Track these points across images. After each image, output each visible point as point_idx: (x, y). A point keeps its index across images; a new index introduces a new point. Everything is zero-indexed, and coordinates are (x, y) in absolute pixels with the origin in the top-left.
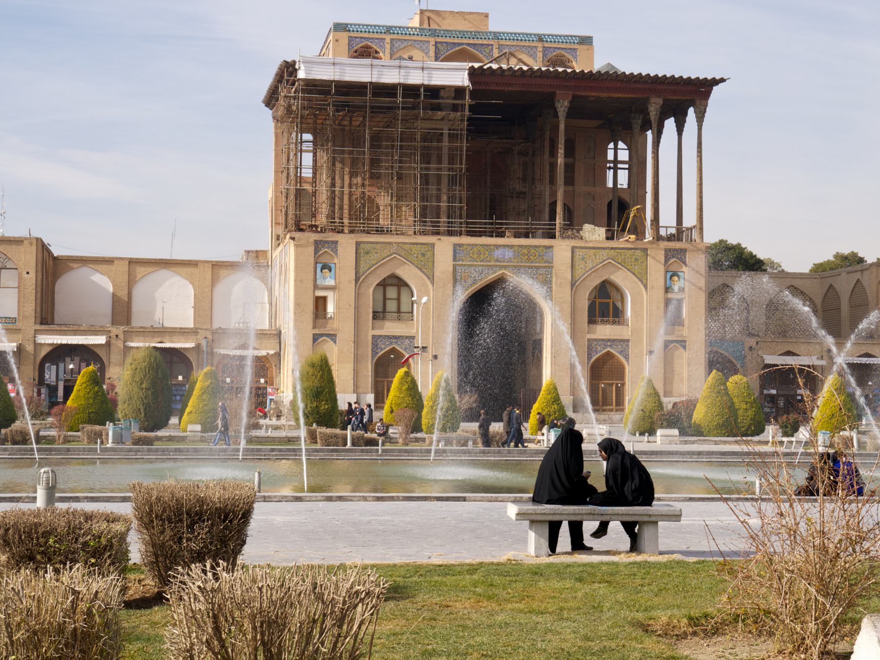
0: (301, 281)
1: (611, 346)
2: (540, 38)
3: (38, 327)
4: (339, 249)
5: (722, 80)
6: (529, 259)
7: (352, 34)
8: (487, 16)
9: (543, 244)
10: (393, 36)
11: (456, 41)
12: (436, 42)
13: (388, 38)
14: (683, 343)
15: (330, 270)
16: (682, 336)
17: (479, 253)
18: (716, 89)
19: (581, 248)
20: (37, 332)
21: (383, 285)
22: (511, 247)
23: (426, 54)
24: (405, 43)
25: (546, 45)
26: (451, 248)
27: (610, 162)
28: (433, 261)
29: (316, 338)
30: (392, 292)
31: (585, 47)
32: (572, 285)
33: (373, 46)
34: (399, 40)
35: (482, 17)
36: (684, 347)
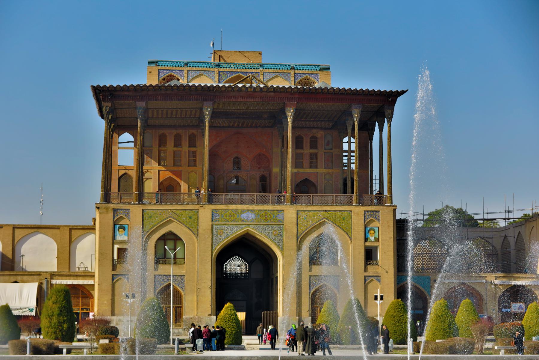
4: (131, 215)
5: (403, 92)
6: (266, 220)
7: (161, 68)
9: (277, 209)
10: (189, 68)
11: (233, 70)
12: (219, 72)
13: (186, 69)
14: (378, 277)
15: (124, 230)
16: (377, 273)
17: (230, 216)
18: (399, 99)
21: (164, 239)
22: (253, 211)
23: (213, 79)
24: (198, 73)
25: (296, 71)
27: (346, 152)
28: (198, 222)
30: (171, 244)
31: (324, 73)
33: (176, 75)
35: (257, 54)
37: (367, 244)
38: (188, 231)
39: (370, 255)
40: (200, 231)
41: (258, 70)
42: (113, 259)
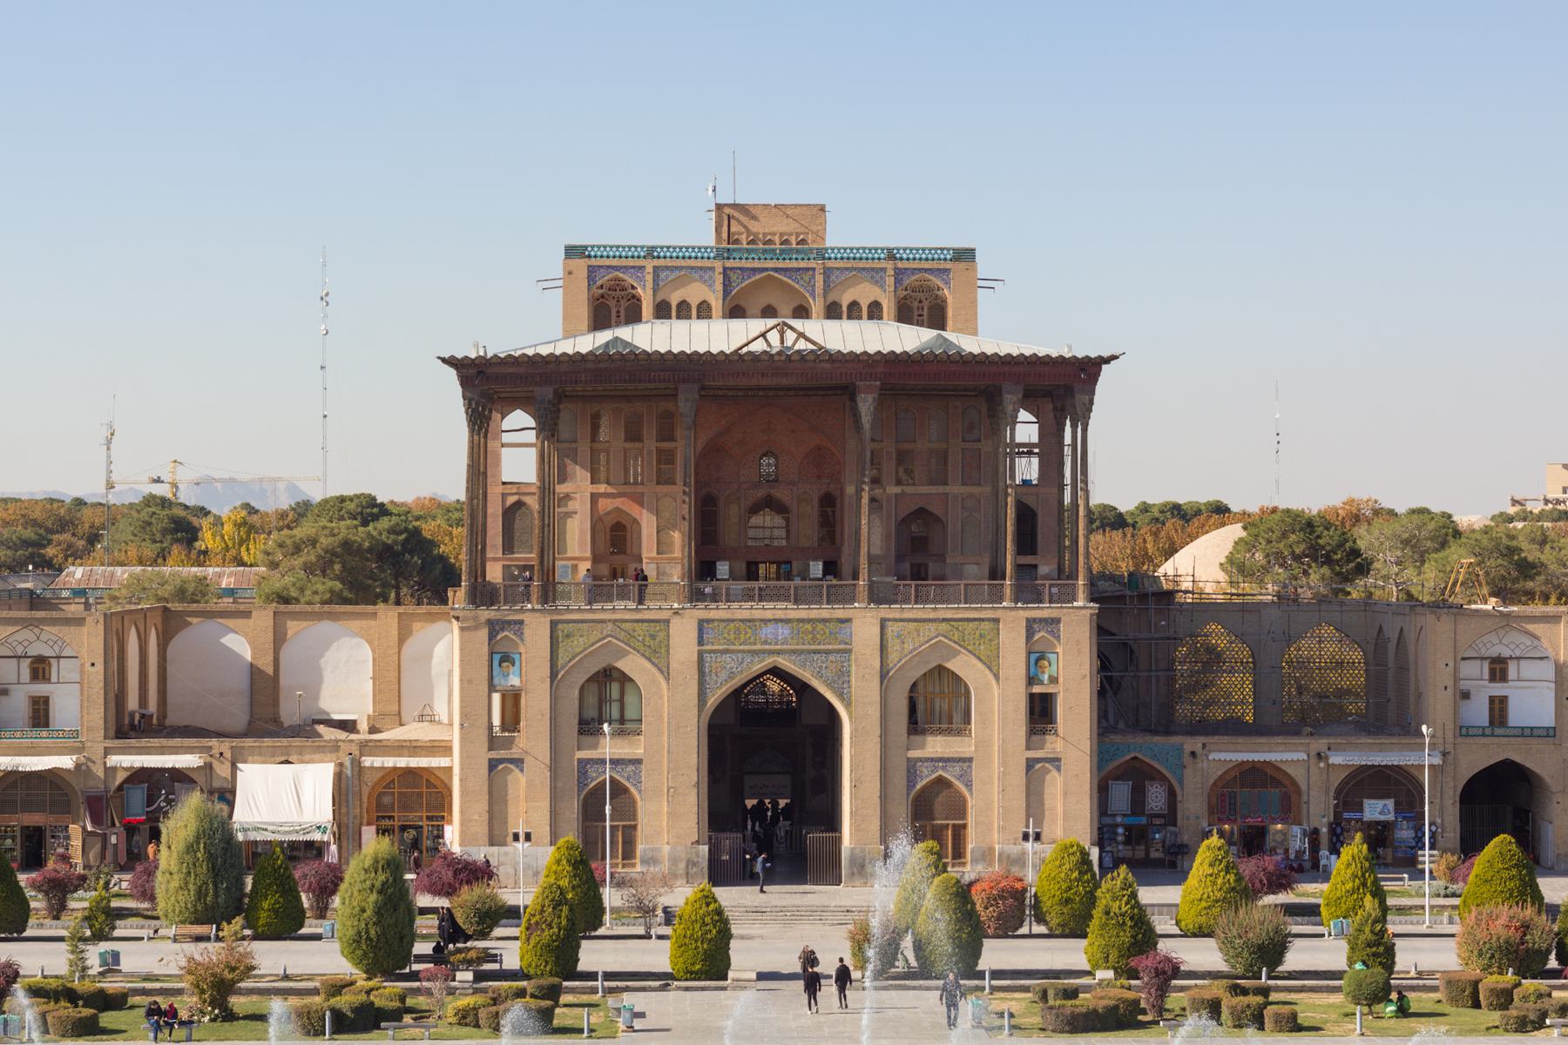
0: (470, 681)
1: (943, 768)
2: (891, 255)
3: (109, 743)
5: (1114, 357)
6: (814, 640)
7: (593, 262)
8: (822, 209)
10: (656, 262)
11: (757, 264)
13: (649, 265)
19: (896, 620)
20: (107, 751)
24: (677, 273)
25: (900, 265)
26: (696, 625)
28: (668, 647)
29: (493, 765)
31: (962, 265)
32: (883, 676)
34: (667, 268)
36: (1058, 769)
37: (1037, 689)
38: (648, 665)
39: (1041, 711)
40: (674, 665)
41: (812, 264)
42: (491, 727)
